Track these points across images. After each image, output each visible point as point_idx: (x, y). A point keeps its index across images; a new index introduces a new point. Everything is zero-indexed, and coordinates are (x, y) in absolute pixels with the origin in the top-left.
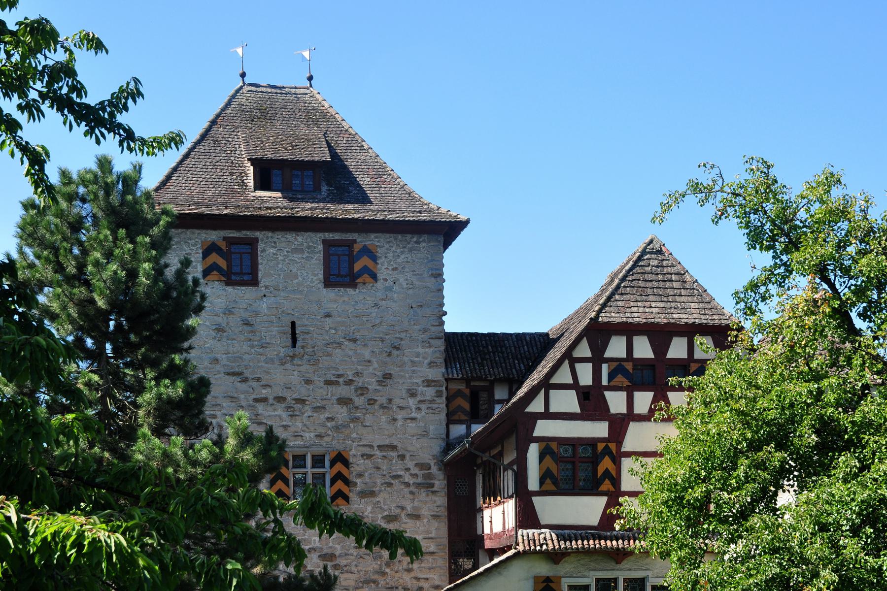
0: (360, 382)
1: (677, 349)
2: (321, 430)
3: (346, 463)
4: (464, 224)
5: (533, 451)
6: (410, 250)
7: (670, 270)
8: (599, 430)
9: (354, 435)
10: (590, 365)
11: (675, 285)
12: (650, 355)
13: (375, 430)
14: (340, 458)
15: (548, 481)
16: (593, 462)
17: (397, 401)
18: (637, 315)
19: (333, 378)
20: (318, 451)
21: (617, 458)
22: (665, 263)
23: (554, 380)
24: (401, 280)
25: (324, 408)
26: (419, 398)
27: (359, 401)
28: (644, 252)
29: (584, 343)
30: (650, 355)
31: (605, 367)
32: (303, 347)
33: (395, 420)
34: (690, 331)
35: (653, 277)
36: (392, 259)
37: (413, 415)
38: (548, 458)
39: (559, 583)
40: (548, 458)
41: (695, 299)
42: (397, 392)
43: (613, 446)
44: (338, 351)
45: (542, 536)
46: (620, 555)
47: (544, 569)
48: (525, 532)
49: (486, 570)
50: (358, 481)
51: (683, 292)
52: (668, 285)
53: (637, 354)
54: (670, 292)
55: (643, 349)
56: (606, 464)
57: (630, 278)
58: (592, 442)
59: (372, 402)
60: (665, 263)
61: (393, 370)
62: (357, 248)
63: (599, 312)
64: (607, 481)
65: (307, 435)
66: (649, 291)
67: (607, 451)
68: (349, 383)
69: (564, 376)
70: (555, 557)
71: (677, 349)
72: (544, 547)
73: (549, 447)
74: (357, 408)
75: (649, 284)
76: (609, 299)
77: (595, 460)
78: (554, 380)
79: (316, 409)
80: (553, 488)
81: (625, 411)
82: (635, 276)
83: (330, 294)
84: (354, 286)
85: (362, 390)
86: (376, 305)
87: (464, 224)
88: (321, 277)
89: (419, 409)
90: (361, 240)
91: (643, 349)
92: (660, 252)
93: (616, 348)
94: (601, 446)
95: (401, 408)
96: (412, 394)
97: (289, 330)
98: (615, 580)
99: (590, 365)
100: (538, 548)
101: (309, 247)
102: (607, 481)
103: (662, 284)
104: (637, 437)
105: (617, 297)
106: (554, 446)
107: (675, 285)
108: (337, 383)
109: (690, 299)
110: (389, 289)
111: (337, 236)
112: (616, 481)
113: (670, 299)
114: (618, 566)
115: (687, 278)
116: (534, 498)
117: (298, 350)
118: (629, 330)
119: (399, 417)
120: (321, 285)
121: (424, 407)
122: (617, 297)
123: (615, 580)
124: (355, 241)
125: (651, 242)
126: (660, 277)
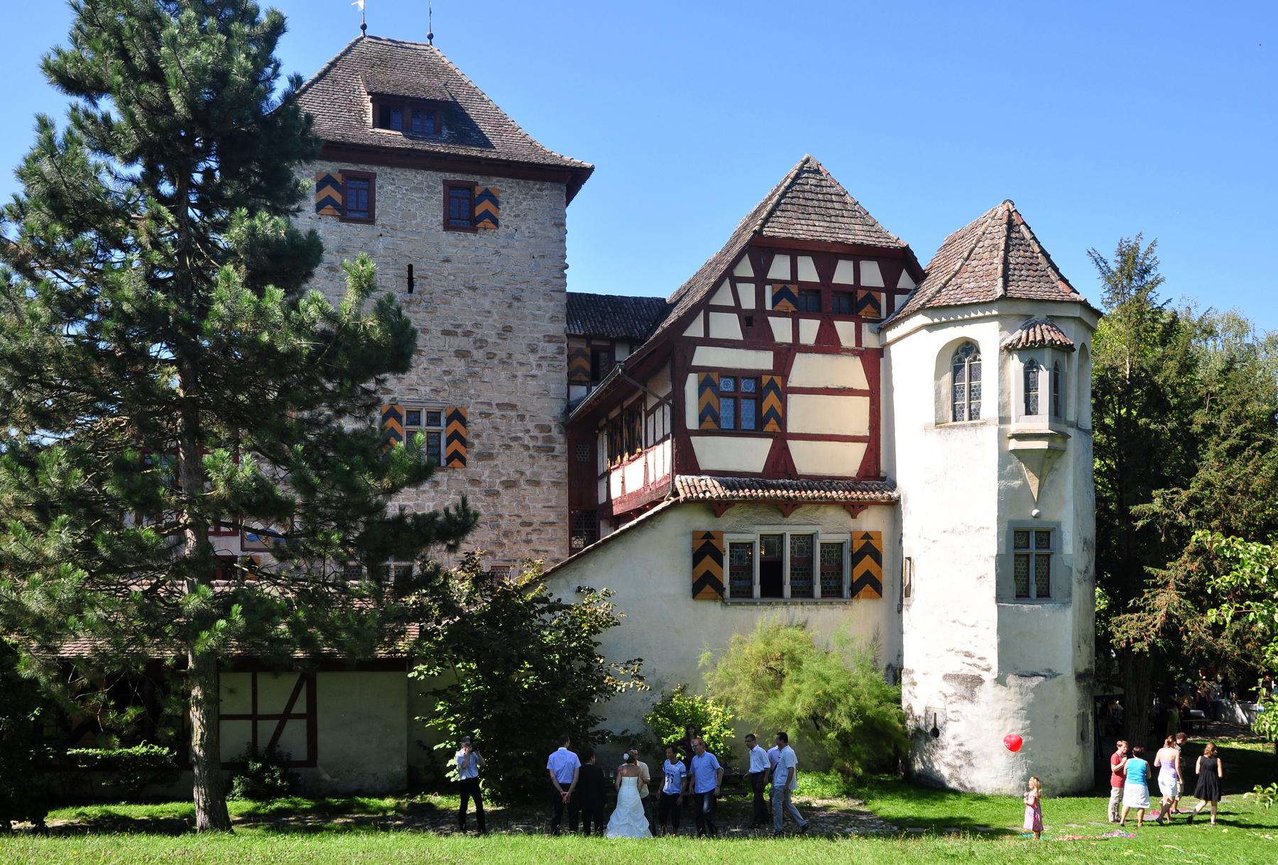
0: (479, 333)
1: (843, 274)
2: (437, 384)
3: (463, 421)
4: (589, 171)
5: (692, 382)
6: (533, 197)
7: (832, 190)
8: (763, 360)
9: (472, 391)
10: (753, 286)
11: (837, 205)
12: (815, 278)
13: (494, 387)
14: (457, 416)
15: (709, 418)
16: (756, 399)
17: (518, 357)
18: (802, 230)
19: (451, 328)
21: (784, 393)
22: (823, 183)
23: (715, 301)
24: (523, 227)
25: (440, 359)
26: (540, 354)
27: (478, 354)
28: (801, 171)
29: (746, 261)
30: (815, 278)
31: (768, 289)
32: (420, 293)
33: (515, 376)
34: (858, 253)
35: (813, 196)
36: (514, 202)
37: (534, 372)
38: (708, 390)
39: (721, 539)
40: (708, 390)
41: (858, 221)
42: (517, 345)
43: (778, 380)
44: (456, 299)
45: (703, 483)
46: (785, 508)
47: (703, 522)
48: (683, 478)
49: (639, 523)
50: (476, 441)
51: (845, 213)
52: (829, 205)
53: (802, 277)
54: (832, 212)
55: (808, 272)
56: (771, 400)
57: (789, 195)
58: (756, 375)
59: (491, 356)
60: (823, 183)
61: (514, 322)
63: (762, 226)
64: (772, 420)
65: (422, 388)
66: (811, 210)
67: (772, 385)
68: (467, 334)
69: (724, 297)
70: (715, 507)
71: (843, 274)
72: (708, 495)
73: (709, 378)
74: (475, 361)
75: (809, 203)
76: (770, 214)
77: (759, 396)
78: (715, 301)
79: (432, 361)
80: (713, 426)
81: (790, 341)
82: (795, 194)
85: (481, 343)
86: (497, 252)
87: (589, 171)
88: (441, 218)
89: (540, 366)
91: (808, 272)
92: (817, 172)
93: (780, 269)
94: (765, 380)
95: (522, 364)
96: (534, 350)
97: (406, 274)
98: (781, 536)
99: (753, 286)
100: (701, 495)
102: (772, 420)
103: (822, 204)
104: (805, 370)
105: (778, 213)
106: (715, 376)
107: (837, 205)
108: (455, 334)
109: (853, 221)
110: (511, 236)
112: (782, 421)
113: (833, 219)
114: (786, 520)
115: (848, 199)
116: (693, 439)
117: (415, 296)
118: (794, 249)
119: (519, 374)
121: (544, 364)
122: (778, 213)
123: (781, 536)
124: (477, 184)
125: (807, 161)
126: (820, 196)
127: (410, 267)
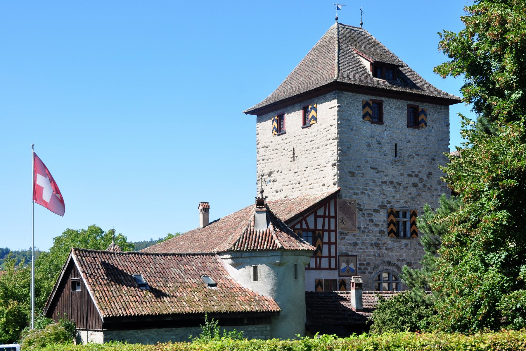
0: (421, 175)
2: (407, 199)
9: (418, 202)
17: (434, 186)
19: (411, 173)
20: (405, 209)
26: (442, 185)
27: (420, 185)
32: (400, 157)
37: (439, 193)
59: (425, 186)
61: (432, 171)
62: (420, 109)
65: (401, 201)
68: (417, 176)
83: (410, 131)
84: (418, 128)
85: (421, 180)
90: (423, 106)
95: (436, 190)
101: (402, 107)
111: (412, 103)
119: (434, 194)
120: (406, 126)
121: (443, 189)
127: (396, 144)
